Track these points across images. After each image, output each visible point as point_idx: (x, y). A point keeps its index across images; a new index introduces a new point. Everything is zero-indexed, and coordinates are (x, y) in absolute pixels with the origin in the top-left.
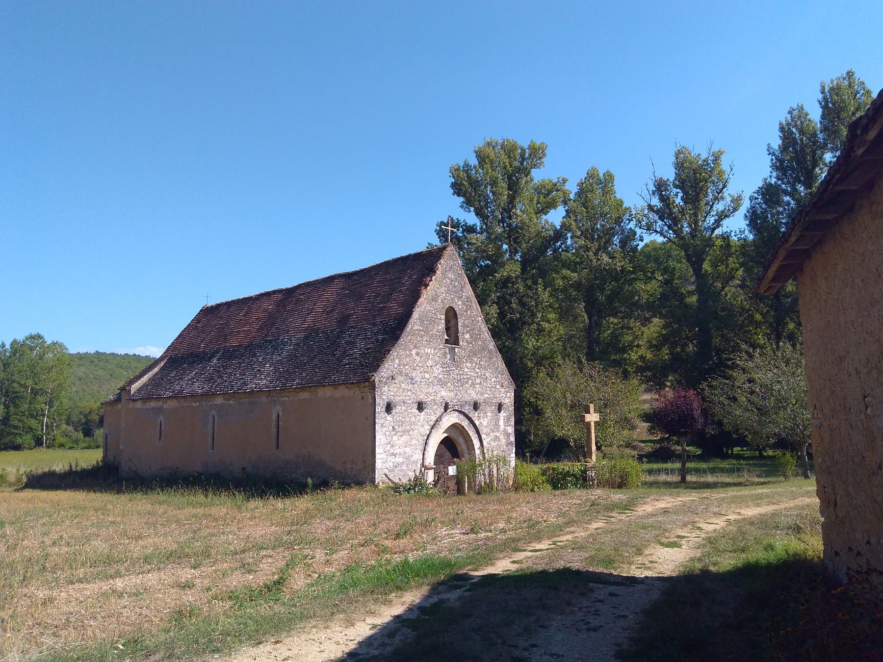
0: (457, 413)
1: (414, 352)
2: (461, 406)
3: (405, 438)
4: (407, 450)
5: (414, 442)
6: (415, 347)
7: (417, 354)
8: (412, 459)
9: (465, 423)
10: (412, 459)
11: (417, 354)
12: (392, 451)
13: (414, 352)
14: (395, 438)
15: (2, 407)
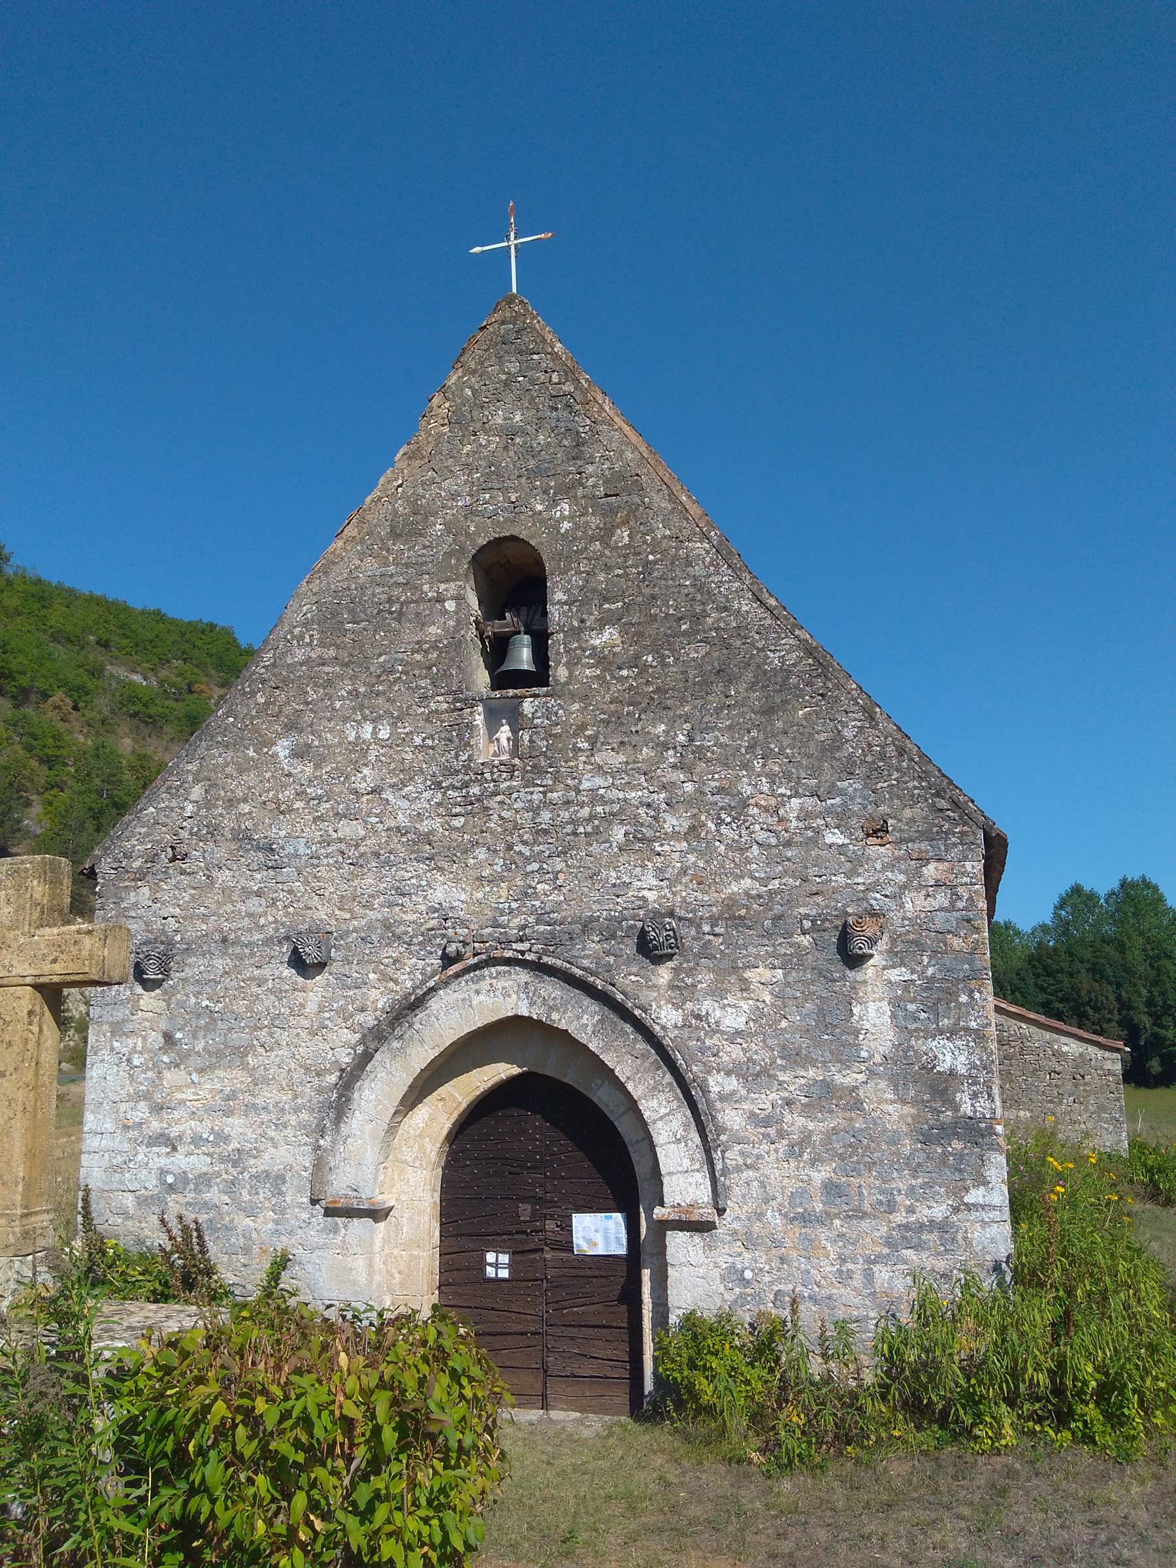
0: (523, 976)
1: (282, 749)
2: (550, 941)
3: (229, 1078)
4: (236, 1125)
5: (268, 1095)
6: (291, 727)
7: (299, 753)
8: (256, 1165)
9: (581, 1020)
10: (256, 1165)
11: (299, 753)
12: (155, 1126)
13: (282, 749)
14: (171, 1077)
15: (531, 1565)
